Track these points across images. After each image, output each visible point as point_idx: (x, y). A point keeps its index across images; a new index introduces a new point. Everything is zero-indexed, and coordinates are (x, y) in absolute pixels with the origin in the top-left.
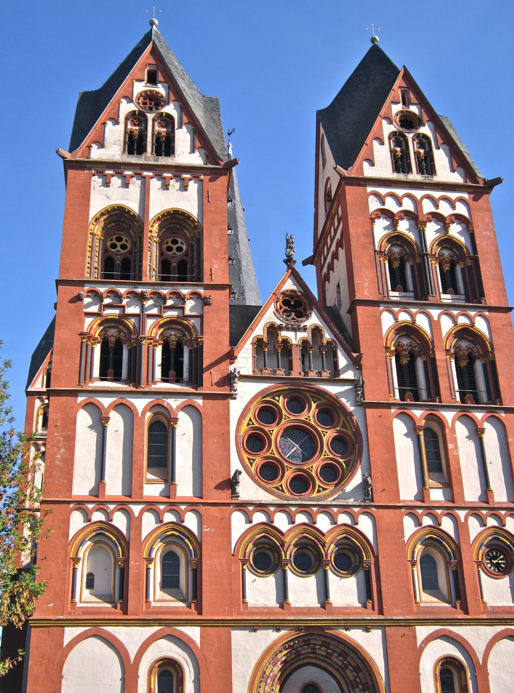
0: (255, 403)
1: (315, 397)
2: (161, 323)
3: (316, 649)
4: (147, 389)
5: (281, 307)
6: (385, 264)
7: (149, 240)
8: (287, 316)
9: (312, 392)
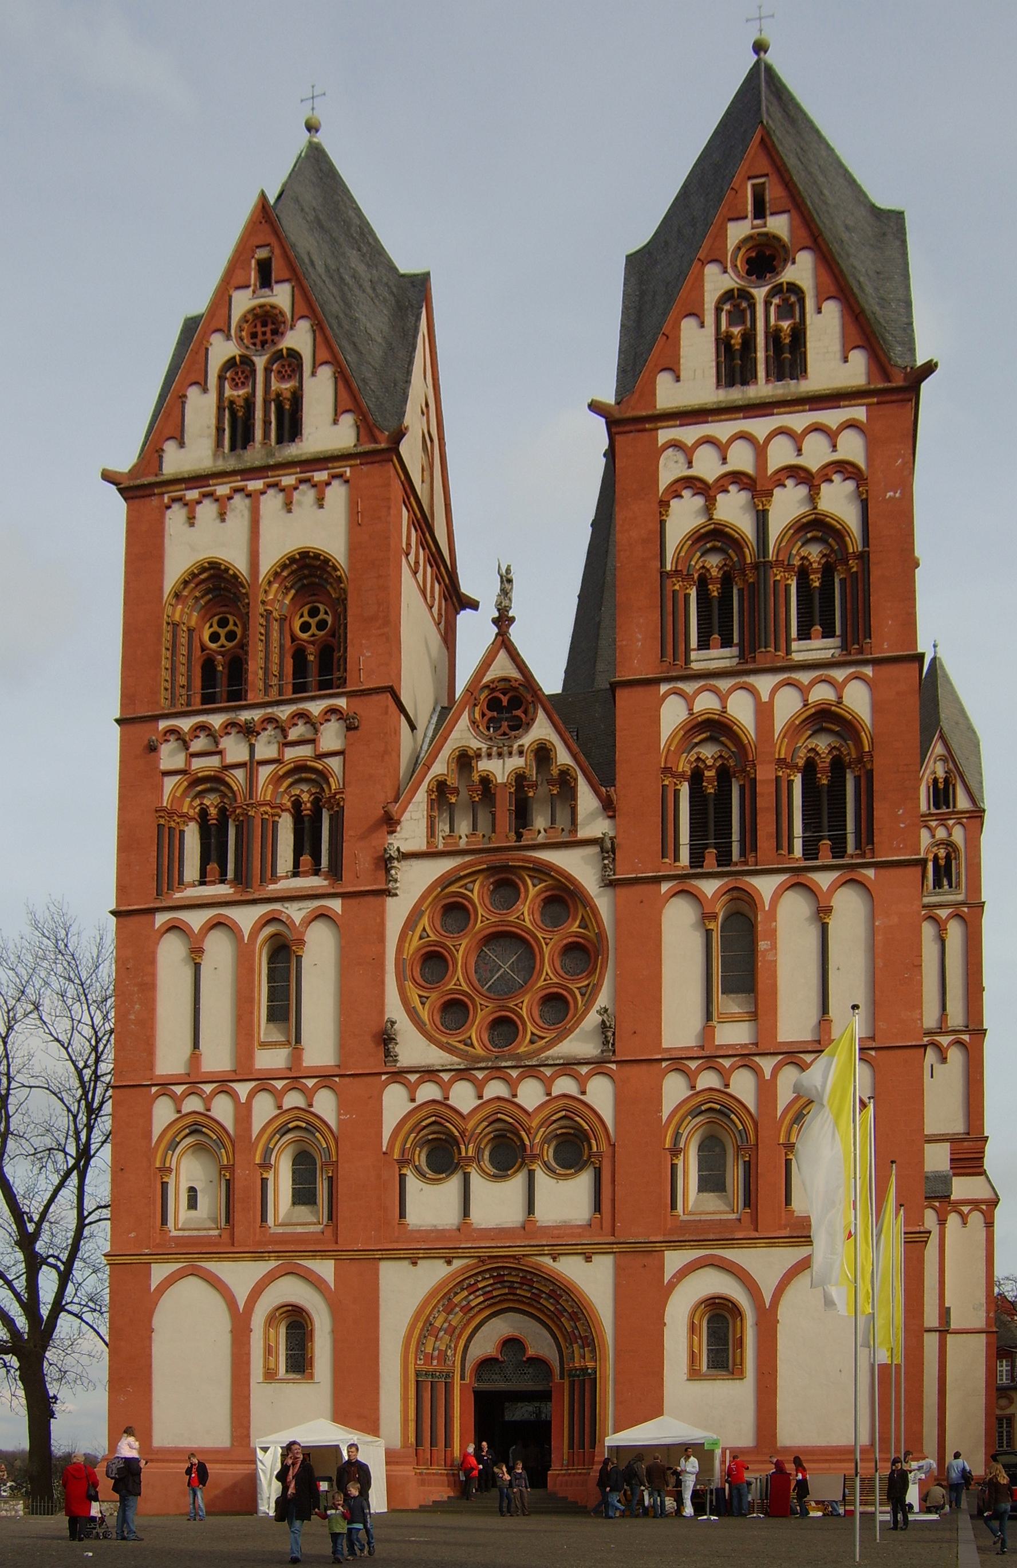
0: (430, 899)
1: (535, 877)
2: (281, 773)
3: (517, 1288)
4: (256, 896)
5: (483, 715)
6: (687, 597)
7: (262, 621)
8: (496, 729)
9: (529, 869)
